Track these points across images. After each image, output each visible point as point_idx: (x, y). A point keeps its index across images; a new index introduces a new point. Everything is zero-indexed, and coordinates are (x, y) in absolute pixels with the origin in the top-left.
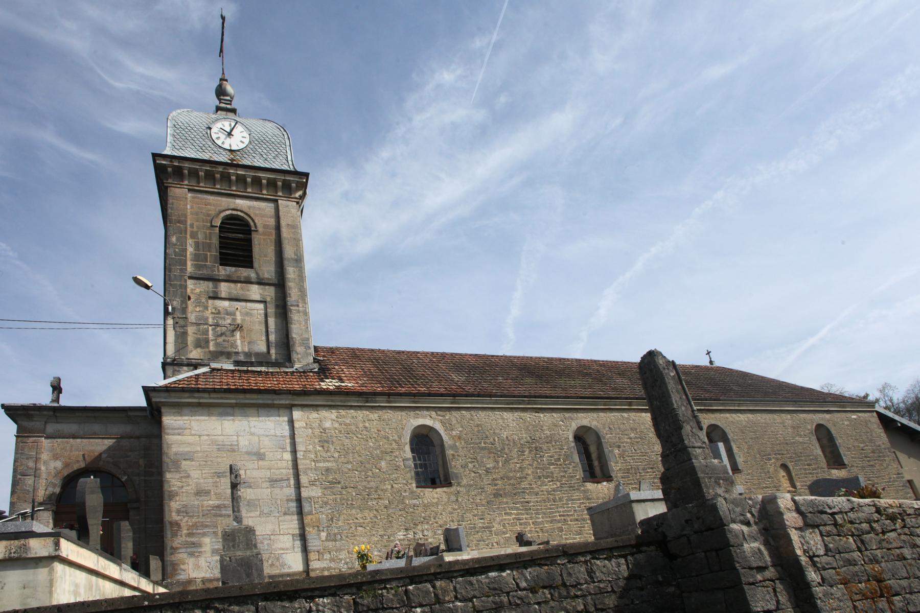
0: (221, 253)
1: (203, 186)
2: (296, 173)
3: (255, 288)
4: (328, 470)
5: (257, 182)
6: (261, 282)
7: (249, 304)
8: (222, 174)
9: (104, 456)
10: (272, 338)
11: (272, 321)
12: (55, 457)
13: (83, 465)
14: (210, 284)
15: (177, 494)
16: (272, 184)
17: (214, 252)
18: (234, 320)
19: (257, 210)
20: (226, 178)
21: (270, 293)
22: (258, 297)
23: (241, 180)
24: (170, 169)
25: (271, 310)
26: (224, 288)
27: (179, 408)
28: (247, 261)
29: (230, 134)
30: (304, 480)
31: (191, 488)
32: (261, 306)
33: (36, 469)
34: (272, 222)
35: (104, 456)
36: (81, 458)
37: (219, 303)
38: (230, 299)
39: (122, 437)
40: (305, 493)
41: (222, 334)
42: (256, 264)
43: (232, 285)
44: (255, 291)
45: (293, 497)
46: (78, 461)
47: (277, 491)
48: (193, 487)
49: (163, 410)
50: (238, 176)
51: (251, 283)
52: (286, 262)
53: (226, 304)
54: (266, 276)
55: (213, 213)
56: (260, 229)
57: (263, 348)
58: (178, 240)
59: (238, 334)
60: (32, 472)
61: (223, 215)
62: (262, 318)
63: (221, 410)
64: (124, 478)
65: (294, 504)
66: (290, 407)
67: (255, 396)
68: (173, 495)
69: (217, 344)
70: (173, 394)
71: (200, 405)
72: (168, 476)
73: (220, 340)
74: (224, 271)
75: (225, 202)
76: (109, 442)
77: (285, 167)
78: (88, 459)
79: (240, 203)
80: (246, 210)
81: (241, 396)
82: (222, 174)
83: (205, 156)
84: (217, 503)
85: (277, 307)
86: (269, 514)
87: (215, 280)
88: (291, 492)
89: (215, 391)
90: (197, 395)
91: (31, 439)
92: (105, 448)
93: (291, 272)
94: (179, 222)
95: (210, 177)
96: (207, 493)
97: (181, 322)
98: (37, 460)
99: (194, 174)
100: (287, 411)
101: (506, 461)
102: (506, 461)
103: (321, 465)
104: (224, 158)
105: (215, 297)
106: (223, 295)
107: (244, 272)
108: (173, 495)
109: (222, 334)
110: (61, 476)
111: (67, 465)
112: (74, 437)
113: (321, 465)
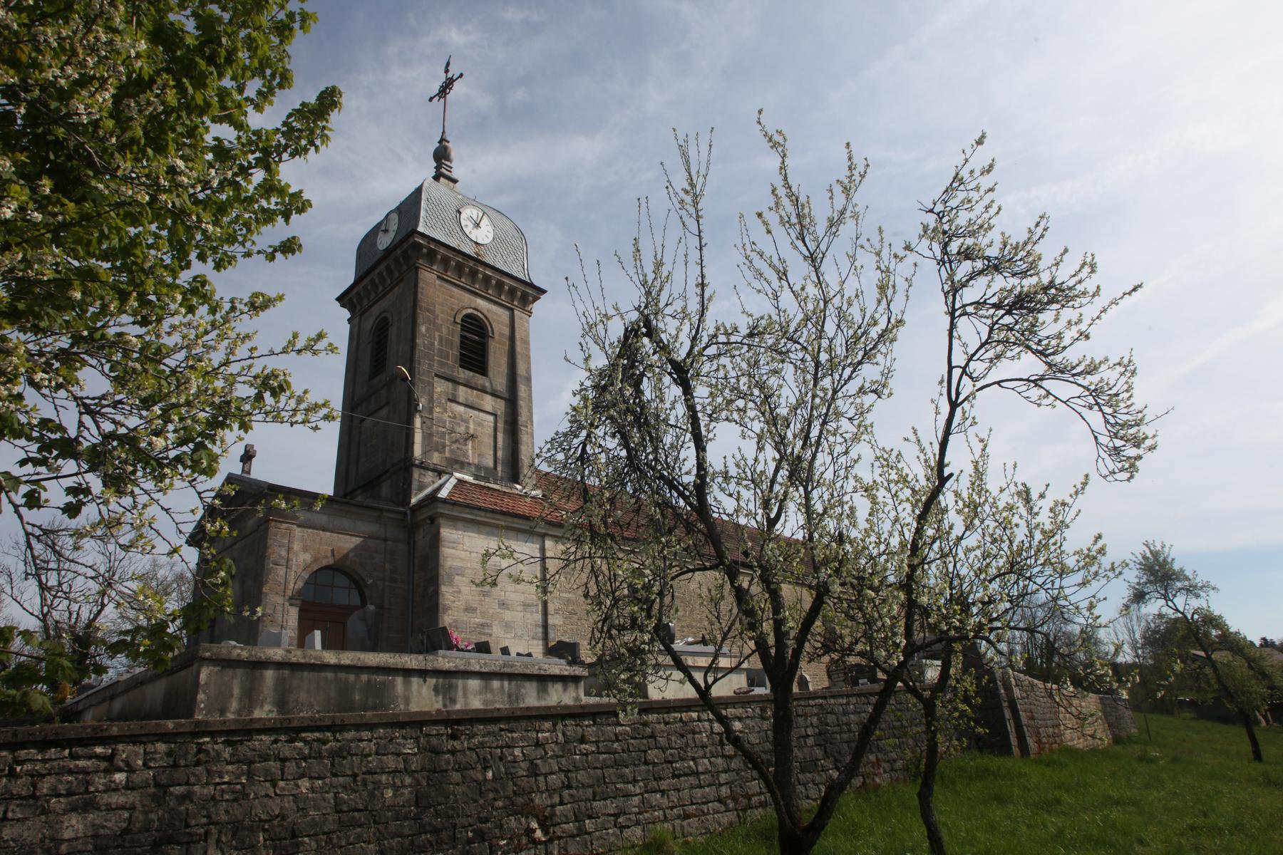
0: (461, 354)
1: (450, 275)
2: (531, 285)
3: (488, 398)
4: (569, 600)
5: (500, 285)
6: (494, 394)
7: (481, 414)
8: (458, 263)
9: (351, 554)
10: (500, 454)
11: (500, 436)
12: (305, 549)
13: (331, 561)
14: (450, 385)
15: (449, 608)
16: (512, 291)
17: (455, 352)
18: (468, 428)
19: (495, 314)
20: (473, 274)
21: (500, 406)
22: (489, 409)
23: (487, 280)
24: (425, 250)
25: (501, 425)
26: (462, 392)
27: (454, 520)
28: (482, 369)
29: (477, 225)
30: (551, 607)
31: (460, 604)
32: (491, 418)
33: (288, 560)
34: (506, 331)
35: (351, 554)
36: (329, 554)
37: (455, 406)
38: (466, 406)
39: (369, 537)
40: (550, 622)
41: (456, 441)
42: (490, 374)
43: (469, 390)
44: (488, 402)
45: (540, 623)
46: (326, 557)
47: (528, 615)
48: (463, 602)
49: (442, 521)
50: (485, 275)
51: (486, 392)
52: (519, 379)
53: (461, 409)
54: (499, 388)
55: (456, 308)
56: (496, 337)
57: (490, 464)
58: (427, 330)
59: (470, 444)
60: (283, 562)
61: (465, 312)
62: (491, 431)
63: (488, 529)
64: (370, 582)
65: (540, 630)
66: (543, 536)
67: (521, 521)
68: (447, 609)
69: (452, 451)
70: (456, 508)
71: (473, 522)
72: (443, 589)
73: (454, 446)
74: (464, 374)
75: (468, 298)
76: (356, 541)
77: (521, 276)
78: (338, 556)
79: (481, 303)
80: (489, 316)
81: (510, 519)
82: (458, 263)
83: (453, 243)
84: (482, 621)
85: (506, 422)
86: (521, 637)
87: (455, 382)
88: (538, 617)
89: (493, 511)
90: (476, 512)
91: (285, 526)
92: (352, 546)
93: (522, 388)
94: (428, 310)
95: (459, 269)
96: (474, 610)
97: (428, 422)
98: (289, 550)
99: (445, 261)
100: (540, 539)
101: (692, 612)
102: (692, 612)
103: (564, 595)
104: (469, 249)
105: (453, 401)
106: (461, 400)
107: (480, 380)
108: (447, 609)
109: (456, 441)
110: (310, 571)
111: (316, 560)
112: (324, 530)
113: (564, 595)
